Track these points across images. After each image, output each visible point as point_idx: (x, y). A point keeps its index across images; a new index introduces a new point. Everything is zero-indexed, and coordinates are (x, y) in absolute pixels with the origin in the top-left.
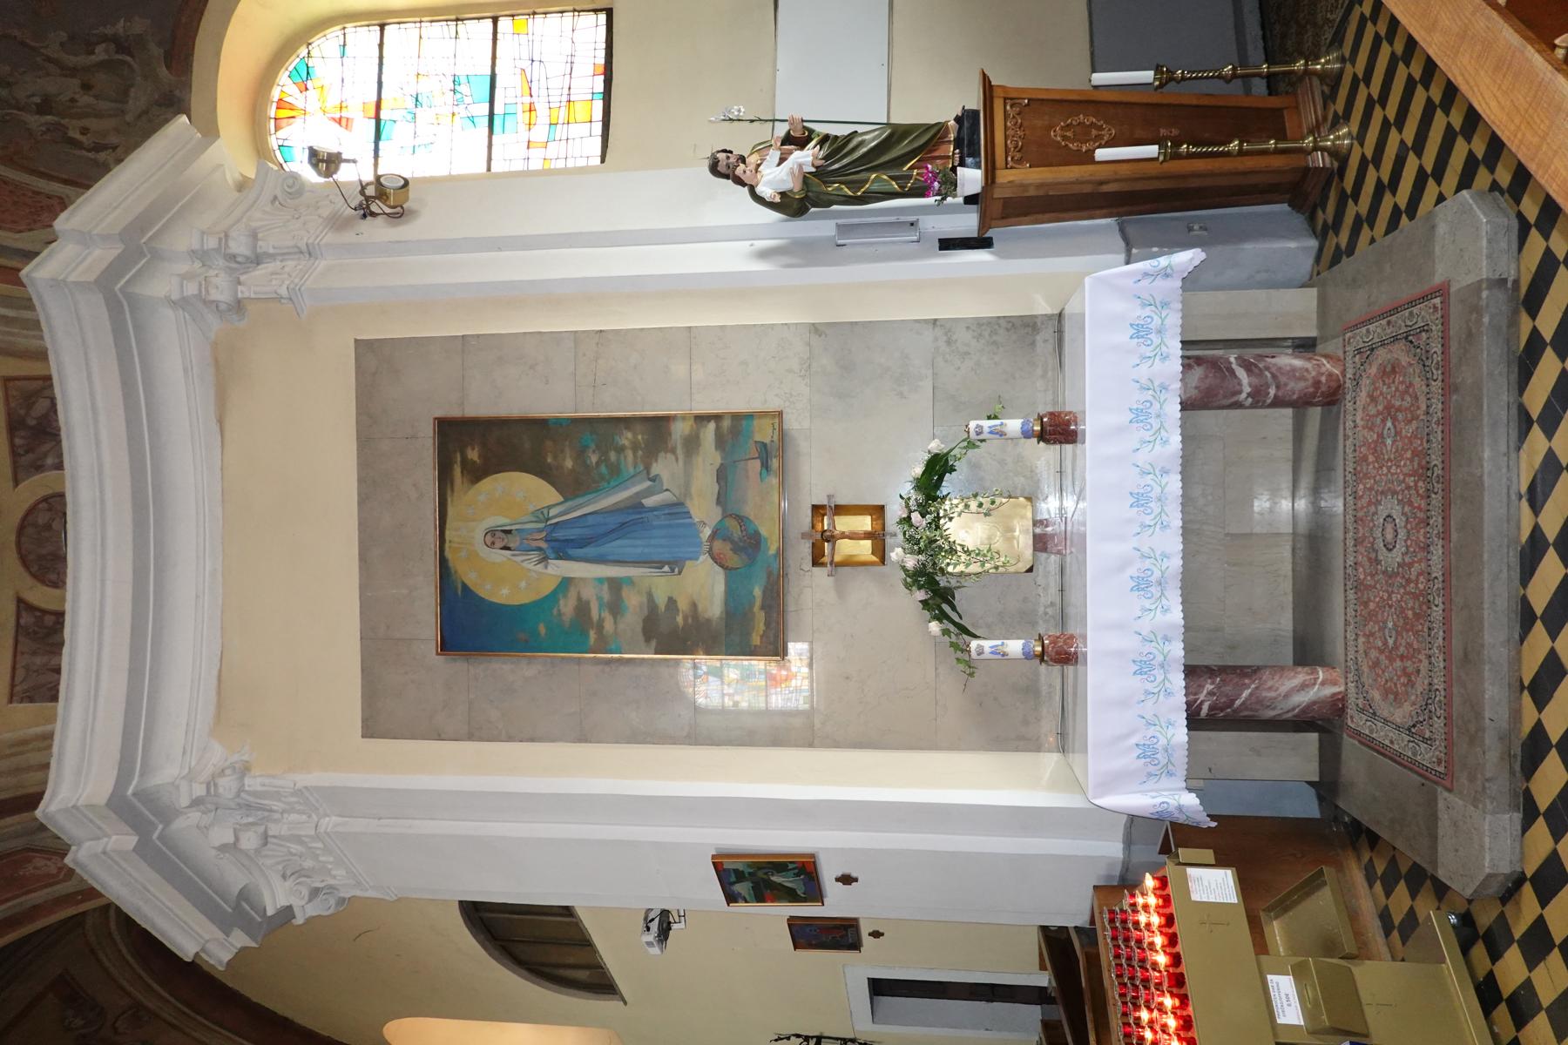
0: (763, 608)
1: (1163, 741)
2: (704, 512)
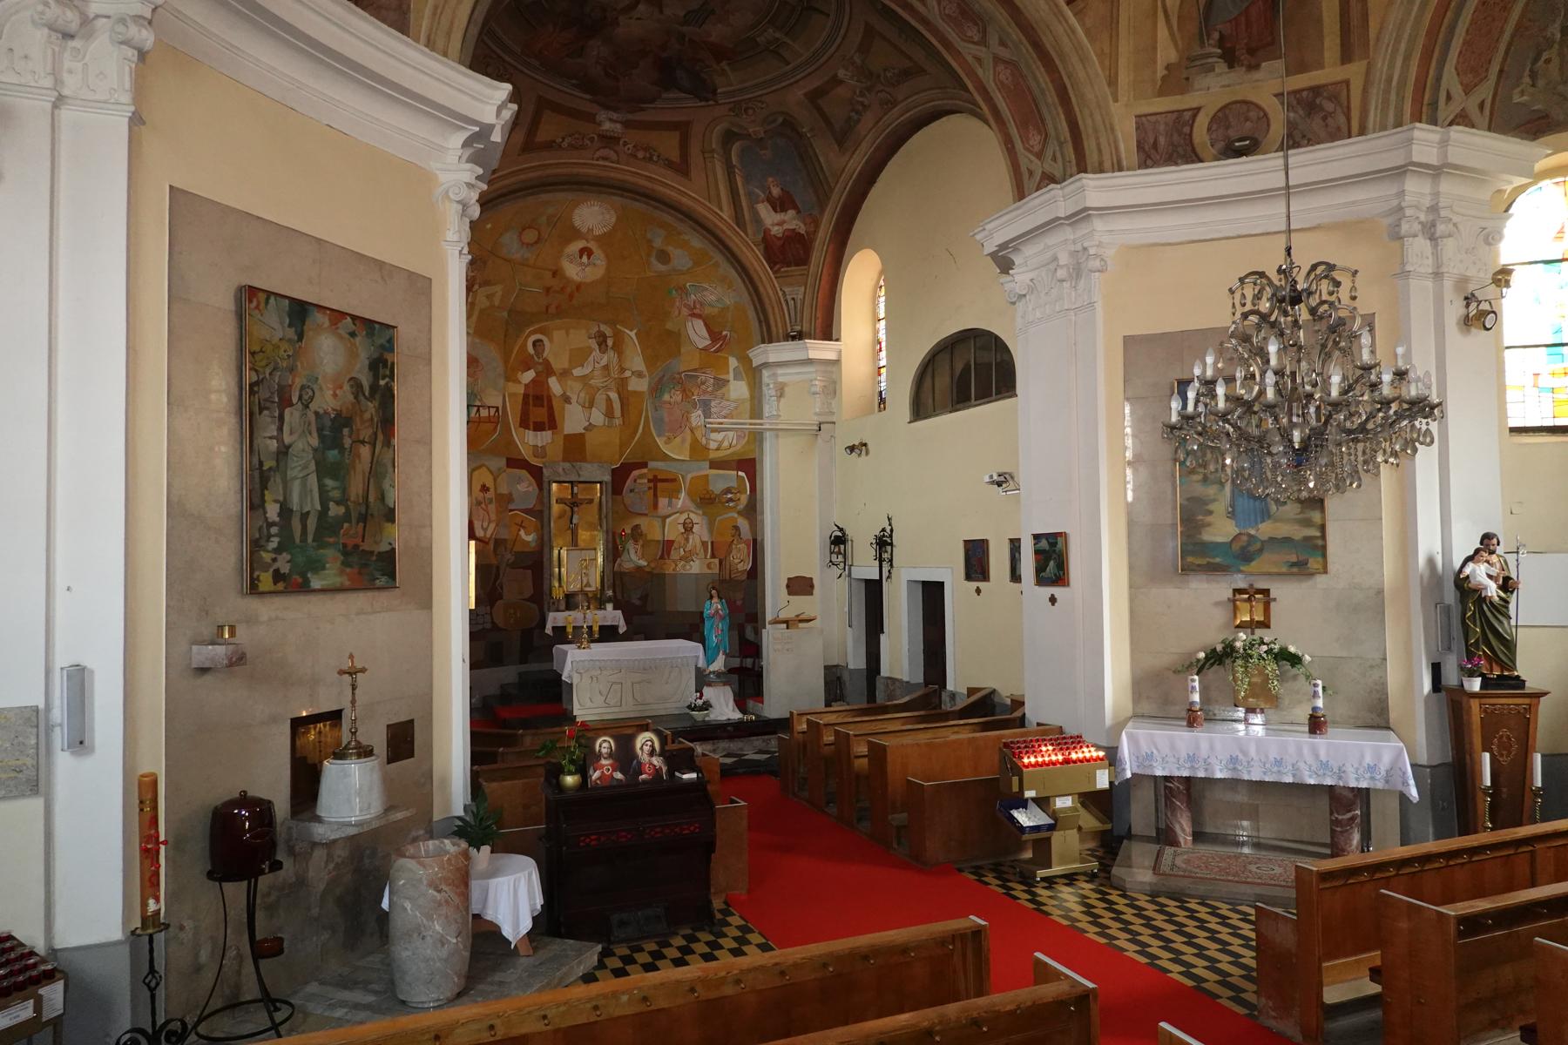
0: (1208, 563)
1: (1155, 764)
2: (1265, 530)
